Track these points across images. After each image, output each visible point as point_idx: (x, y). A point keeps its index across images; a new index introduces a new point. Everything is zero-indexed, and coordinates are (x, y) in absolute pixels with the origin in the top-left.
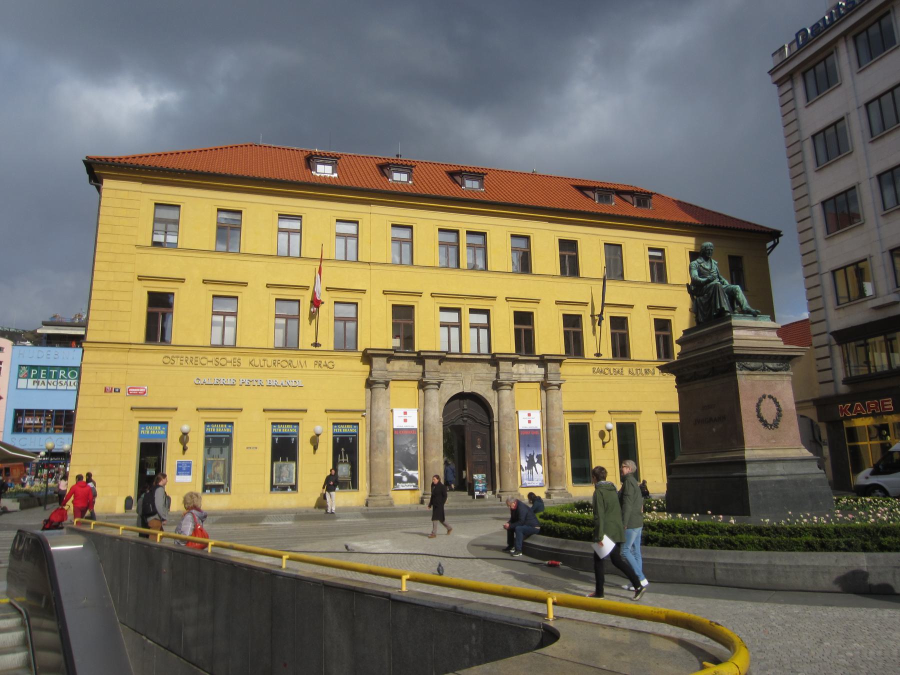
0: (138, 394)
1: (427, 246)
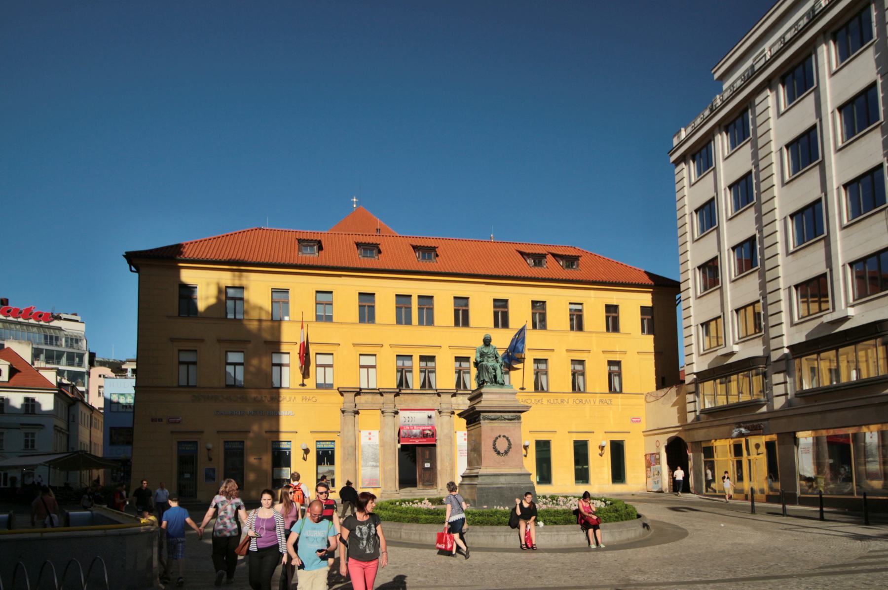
0: (175, 422)
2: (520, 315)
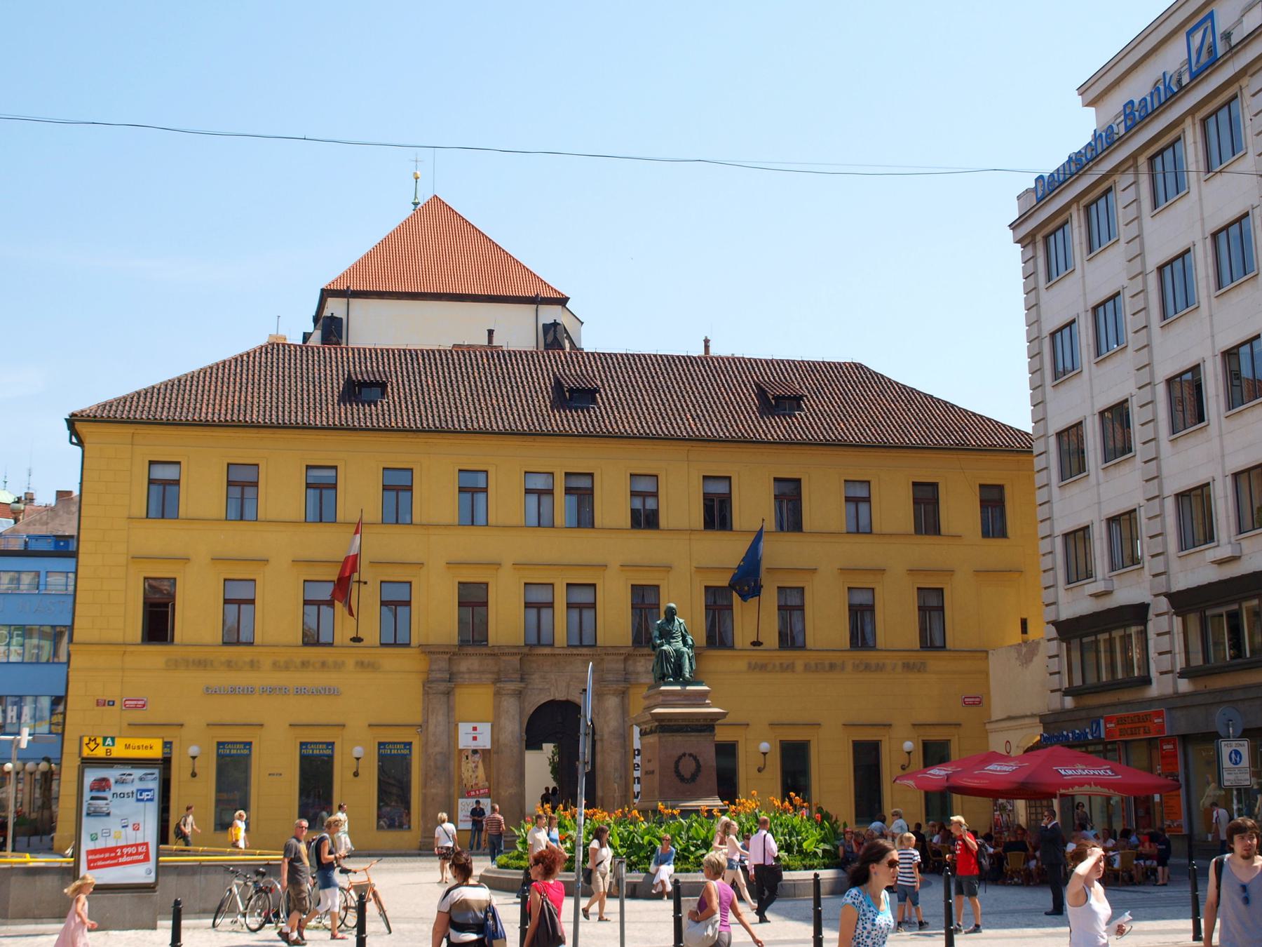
0: (136, 707)
1: (506, 499)
2: (753, 505)
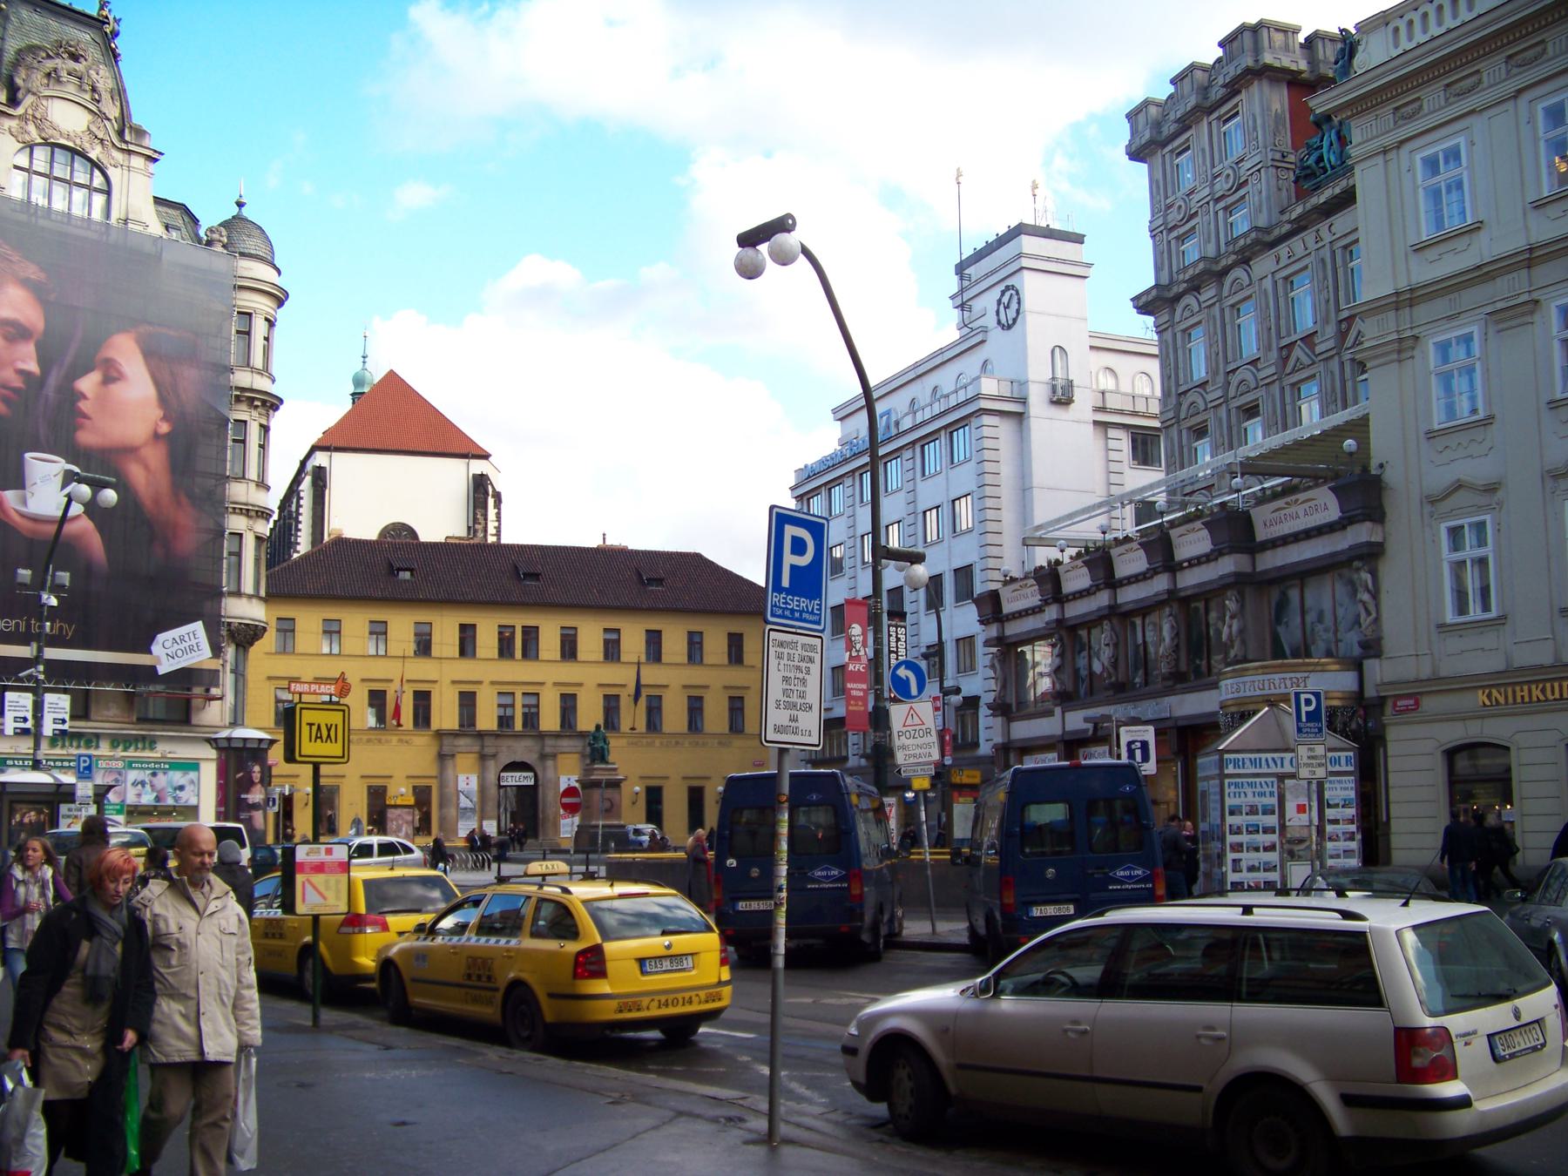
1: (487, 639)
